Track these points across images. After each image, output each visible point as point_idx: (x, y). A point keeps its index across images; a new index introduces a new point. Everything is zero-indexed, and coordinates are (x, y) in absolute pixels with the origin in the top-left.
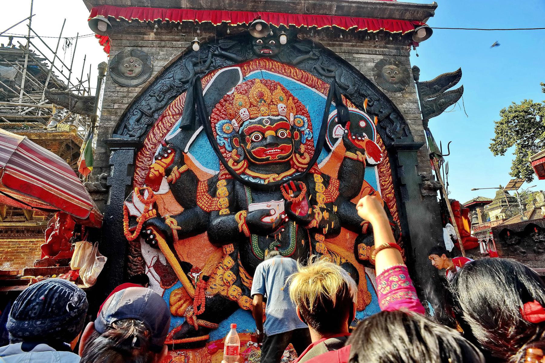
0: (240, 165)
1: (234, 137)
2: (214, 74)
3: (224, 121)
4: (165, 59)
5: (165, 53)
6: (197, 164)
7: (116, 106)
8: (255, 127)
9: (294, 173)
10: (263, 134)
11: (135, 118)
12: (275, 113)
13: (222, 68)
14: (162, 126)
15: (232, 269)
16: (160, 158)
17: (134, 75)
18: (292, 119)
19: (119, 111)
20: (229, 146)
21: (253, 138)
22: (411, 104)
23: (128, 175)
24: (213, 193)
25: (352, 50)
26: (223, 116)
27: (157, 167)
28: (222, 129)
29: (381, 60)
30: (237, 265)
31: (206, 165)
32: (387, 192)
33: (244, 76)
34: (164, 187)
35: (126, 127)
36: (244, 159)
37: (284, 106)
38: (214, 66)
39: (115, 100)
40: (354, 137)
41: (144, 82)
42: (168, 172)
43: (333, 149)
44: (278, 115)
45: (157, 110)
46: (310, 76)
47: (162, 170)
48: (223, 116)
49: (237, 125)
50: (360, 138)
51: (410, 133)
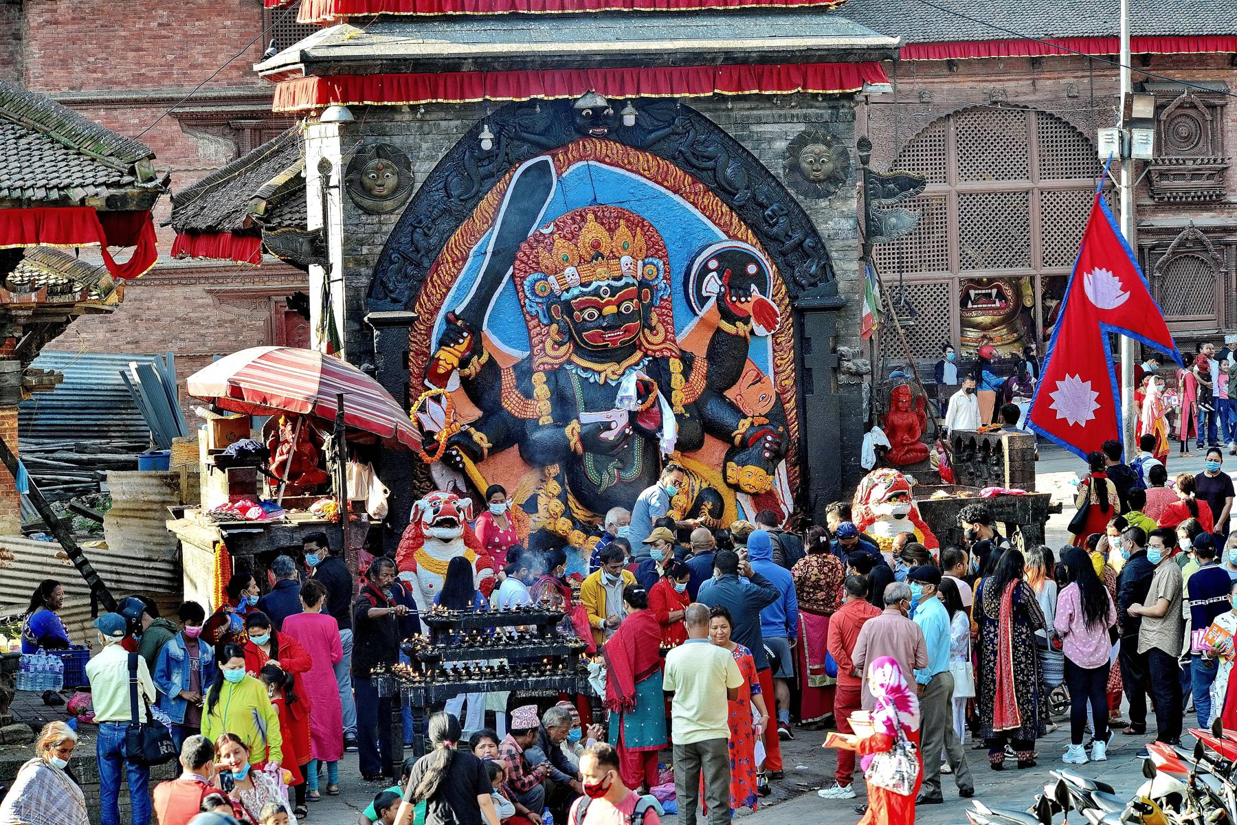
0: (564, 349)
3: (536, 276)
4: (432, 158)
5: (429, 145)
7: (365, 251)
9: (641, 359)
10: (600, 311)
15: (559, 497)
19: (370, 259)
22: (843, 221)
24: (528, 394)
25: (748, 117)
26: (534, 265)
27: (448, 357)
30: (565, 492)
31: (507, 342)
32: (783, 376)
33: (559, 175)
35: (382, 282)
36: (569, 340)
39: (363, 239)
40: (734, 299)
42: (464, 363)
43: (701, 314)
46: (672, 167)
48: (534, 265)
51: (834, 275)
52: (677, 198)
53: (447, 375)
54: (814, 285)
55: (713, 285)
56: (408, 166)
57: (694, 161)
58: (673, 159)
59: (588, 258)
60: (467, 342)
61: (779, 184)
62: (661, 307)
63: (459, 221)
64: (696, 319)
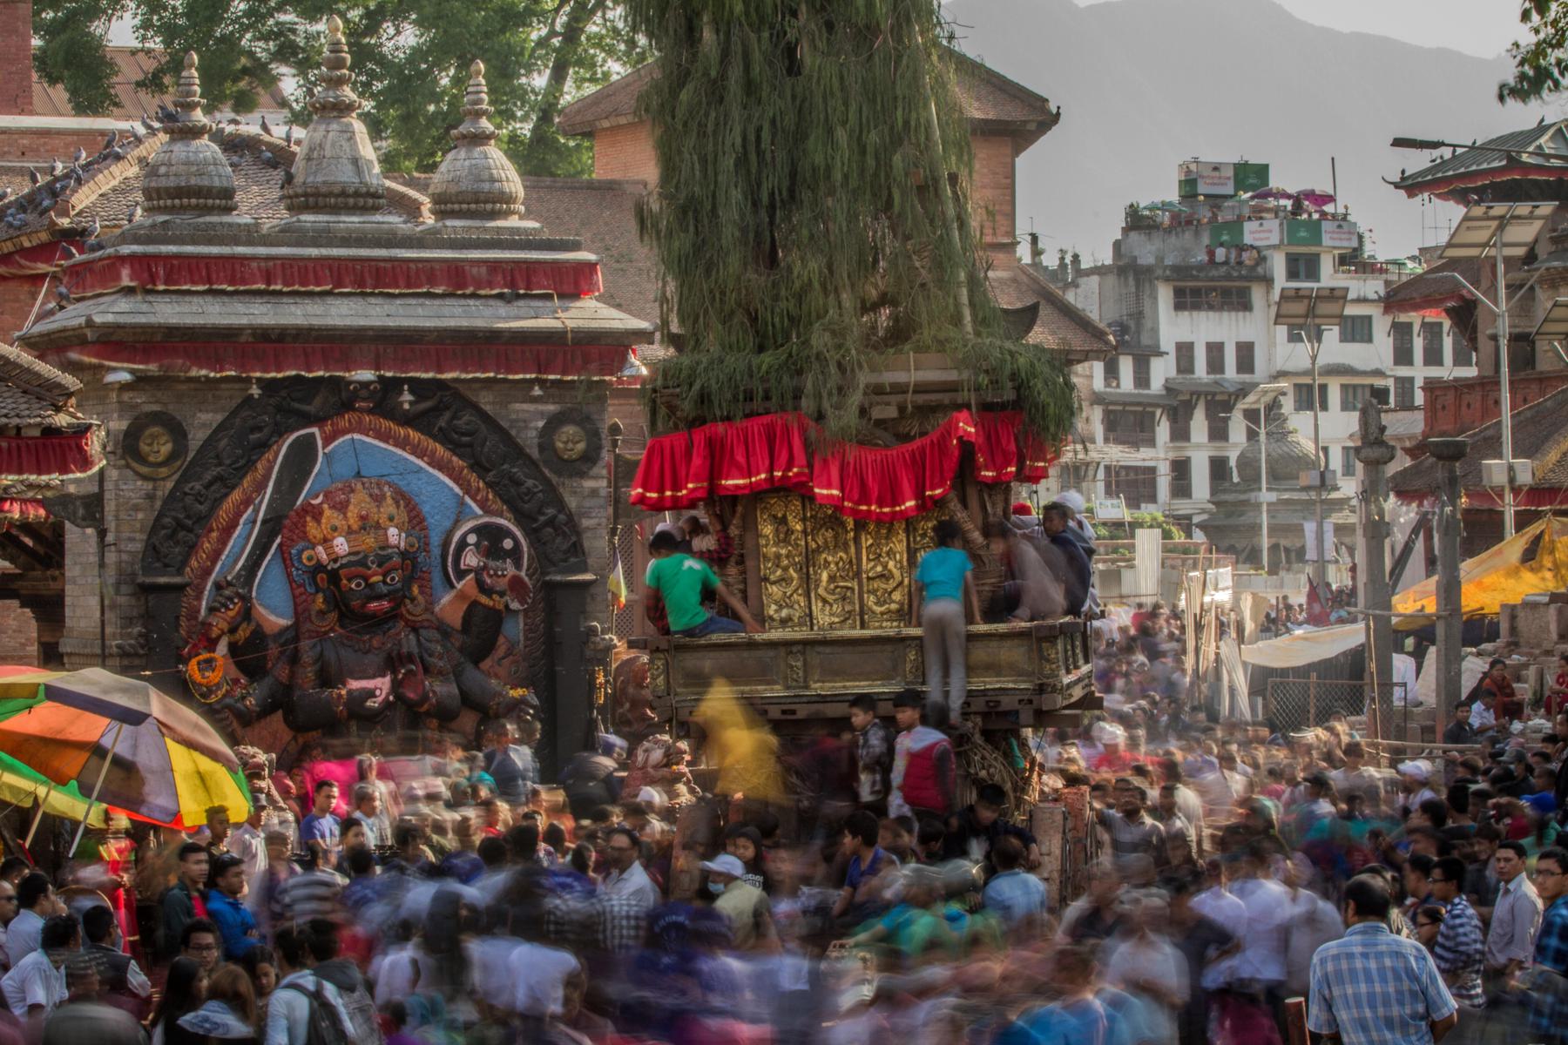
6: (261, 609)
10: (366, 579)
17: (160, 459)
18: (402, 545)
27: (219, 623)
31: (274, 611)
34: (222, 648)
35: (154, 547)
42: (233, 630)
43: (459, 586)
47: (225, 626)
53: (219, 638)
54: (565, 560)
55: (471, 559)
56: (184, 435)
58: (435, 438)
59: (355, 527)
61: (533, 463)
64: (453, 593)
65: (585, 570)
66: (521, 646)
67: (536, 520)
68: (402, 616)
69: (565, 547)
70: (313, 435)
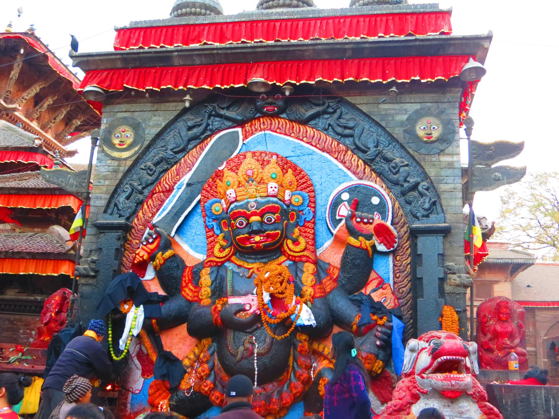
1: (223, 219)
2: (211, 140)
3: (216, 199)
6: (186, 247)
8: (239, 212)
11: (124, 195)
12: (265, 194)
13: (220, 130)
14: (152, 204)
16: (145, 243)
17: (124, 147)
18: (287, 198)
20: (217, 228)
21: (238, 225)
23: (116, 259)
26: (215, 194)
27: (142, 254)
28: (211, 209)
29: (416, 112)
31: (196, 248)
35: (116, 205)
37: (276, 185)
38: (211, 130)
41: (135, 153)
43: (334, 232)
44: (268, 196)
45: (147, 186)
46: (323, 135)
48: (215, 194)
49: (225, 206)
50: (365, 220)
51: (442, 210)
52: (325, 154)
54: (427, 216)
55: (344, 211)
57: (339, 130)
60: (155, 244)
62: (304, 226)
63: (172, 166)
65: (445, 222)
66: (391, 282)
67: (402, 186)
68: (283, 253)
69: (427, 206)
70: (237, 132)
